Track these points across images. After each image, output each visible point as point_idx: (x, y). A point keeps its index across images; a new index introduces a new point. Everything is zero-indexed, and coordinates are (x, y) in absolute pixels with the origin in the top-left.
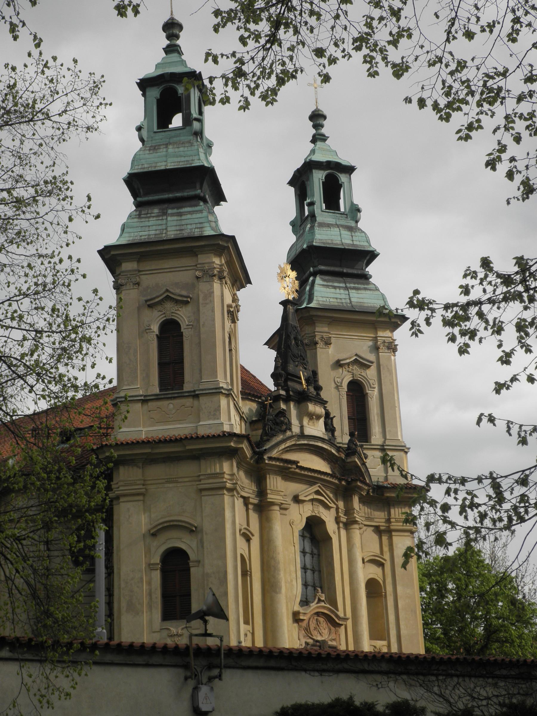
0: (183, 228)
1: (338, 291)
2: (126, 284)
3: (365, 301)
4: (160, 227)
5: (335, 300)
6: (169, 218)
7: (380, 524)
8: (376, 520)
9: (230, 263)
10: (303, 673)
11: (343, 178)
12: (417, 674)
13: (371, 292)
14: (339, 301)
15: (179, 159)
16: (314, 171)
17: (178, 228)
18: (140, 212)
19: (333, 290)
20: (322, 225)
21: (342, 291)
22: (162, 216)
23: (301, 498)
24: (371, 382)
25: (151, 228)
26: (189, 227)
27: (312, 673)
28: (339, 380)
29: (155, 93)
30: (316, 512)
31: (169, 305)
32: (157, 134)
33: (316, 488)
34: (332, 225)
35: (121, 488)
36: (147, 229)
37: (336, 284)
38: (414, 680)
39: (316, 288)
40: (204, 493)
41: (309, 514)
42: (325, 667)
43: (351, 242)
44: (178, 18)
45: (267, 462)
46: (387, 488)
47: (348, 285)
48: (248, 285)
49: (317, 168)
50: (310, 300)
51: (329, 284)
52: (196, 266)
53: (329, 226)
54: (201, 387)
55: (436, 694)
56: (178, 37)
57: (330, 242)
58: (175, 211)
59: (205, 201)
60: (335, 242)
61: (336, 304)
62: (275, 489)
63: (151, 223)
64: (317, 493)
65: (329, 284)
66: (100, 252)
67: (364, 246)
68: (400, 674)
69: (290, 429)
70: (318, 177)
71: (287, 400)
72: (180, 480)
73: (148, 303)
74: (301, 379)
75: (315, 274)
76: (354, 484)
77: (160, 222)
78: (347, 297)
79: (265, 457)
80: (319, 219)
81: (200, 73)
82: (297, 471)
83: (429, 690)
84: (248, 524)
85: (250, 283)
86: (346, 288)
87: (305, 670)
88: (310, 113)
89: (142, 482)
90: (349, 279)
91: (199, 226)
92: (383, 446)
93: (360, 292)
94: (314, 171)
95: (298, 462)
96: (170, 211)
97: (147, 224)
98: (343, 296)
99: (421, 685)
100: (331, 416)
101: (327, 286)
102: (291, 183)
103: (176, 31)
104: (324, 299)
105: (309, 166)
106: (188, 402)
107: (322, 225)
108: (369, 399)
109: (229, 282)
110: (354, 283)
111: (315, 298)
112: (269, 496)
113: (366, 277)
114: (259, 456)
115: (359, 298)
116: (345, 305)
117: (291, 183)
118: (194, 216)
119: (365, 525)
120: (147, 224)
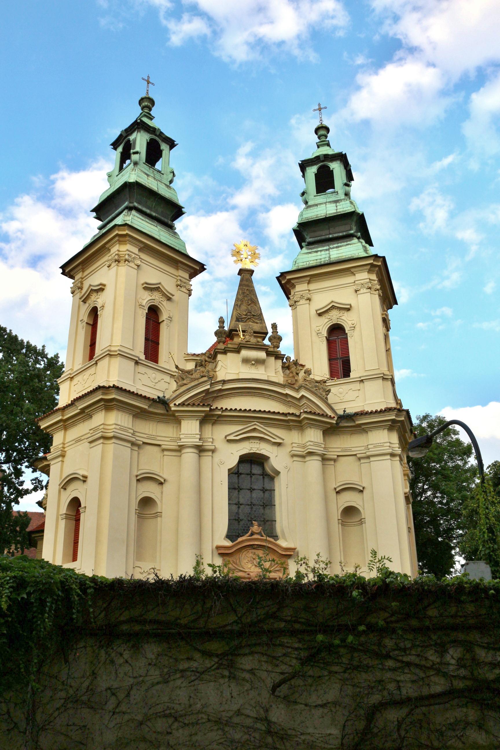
1: (319, 253)
3: (343, 254)
5: (315, 261)
8: (353, 449)
13: (354, 245)
14: (318, 261)
16: (307, 168)
19: (315, 254)
21: (323, 253)
24: (350, 323)
37: (320, 249)
43: (335, 211)
45: (173, 409)
47: (331, 246)
49: (309, 166)
53: (316, 205)
60: (319, 215)
64: (254, 430)
65: (313, 250)
67: (346, 211)
70: (312, 171)
72: (82, 438)
79: (172, 405)
86: (328, 250)
92: (360, 377)
93: (340, 248)
98: (323, 256)
101: (310, 253)
103: (145, 103)
104: (305, 263)
110: (338, 243)
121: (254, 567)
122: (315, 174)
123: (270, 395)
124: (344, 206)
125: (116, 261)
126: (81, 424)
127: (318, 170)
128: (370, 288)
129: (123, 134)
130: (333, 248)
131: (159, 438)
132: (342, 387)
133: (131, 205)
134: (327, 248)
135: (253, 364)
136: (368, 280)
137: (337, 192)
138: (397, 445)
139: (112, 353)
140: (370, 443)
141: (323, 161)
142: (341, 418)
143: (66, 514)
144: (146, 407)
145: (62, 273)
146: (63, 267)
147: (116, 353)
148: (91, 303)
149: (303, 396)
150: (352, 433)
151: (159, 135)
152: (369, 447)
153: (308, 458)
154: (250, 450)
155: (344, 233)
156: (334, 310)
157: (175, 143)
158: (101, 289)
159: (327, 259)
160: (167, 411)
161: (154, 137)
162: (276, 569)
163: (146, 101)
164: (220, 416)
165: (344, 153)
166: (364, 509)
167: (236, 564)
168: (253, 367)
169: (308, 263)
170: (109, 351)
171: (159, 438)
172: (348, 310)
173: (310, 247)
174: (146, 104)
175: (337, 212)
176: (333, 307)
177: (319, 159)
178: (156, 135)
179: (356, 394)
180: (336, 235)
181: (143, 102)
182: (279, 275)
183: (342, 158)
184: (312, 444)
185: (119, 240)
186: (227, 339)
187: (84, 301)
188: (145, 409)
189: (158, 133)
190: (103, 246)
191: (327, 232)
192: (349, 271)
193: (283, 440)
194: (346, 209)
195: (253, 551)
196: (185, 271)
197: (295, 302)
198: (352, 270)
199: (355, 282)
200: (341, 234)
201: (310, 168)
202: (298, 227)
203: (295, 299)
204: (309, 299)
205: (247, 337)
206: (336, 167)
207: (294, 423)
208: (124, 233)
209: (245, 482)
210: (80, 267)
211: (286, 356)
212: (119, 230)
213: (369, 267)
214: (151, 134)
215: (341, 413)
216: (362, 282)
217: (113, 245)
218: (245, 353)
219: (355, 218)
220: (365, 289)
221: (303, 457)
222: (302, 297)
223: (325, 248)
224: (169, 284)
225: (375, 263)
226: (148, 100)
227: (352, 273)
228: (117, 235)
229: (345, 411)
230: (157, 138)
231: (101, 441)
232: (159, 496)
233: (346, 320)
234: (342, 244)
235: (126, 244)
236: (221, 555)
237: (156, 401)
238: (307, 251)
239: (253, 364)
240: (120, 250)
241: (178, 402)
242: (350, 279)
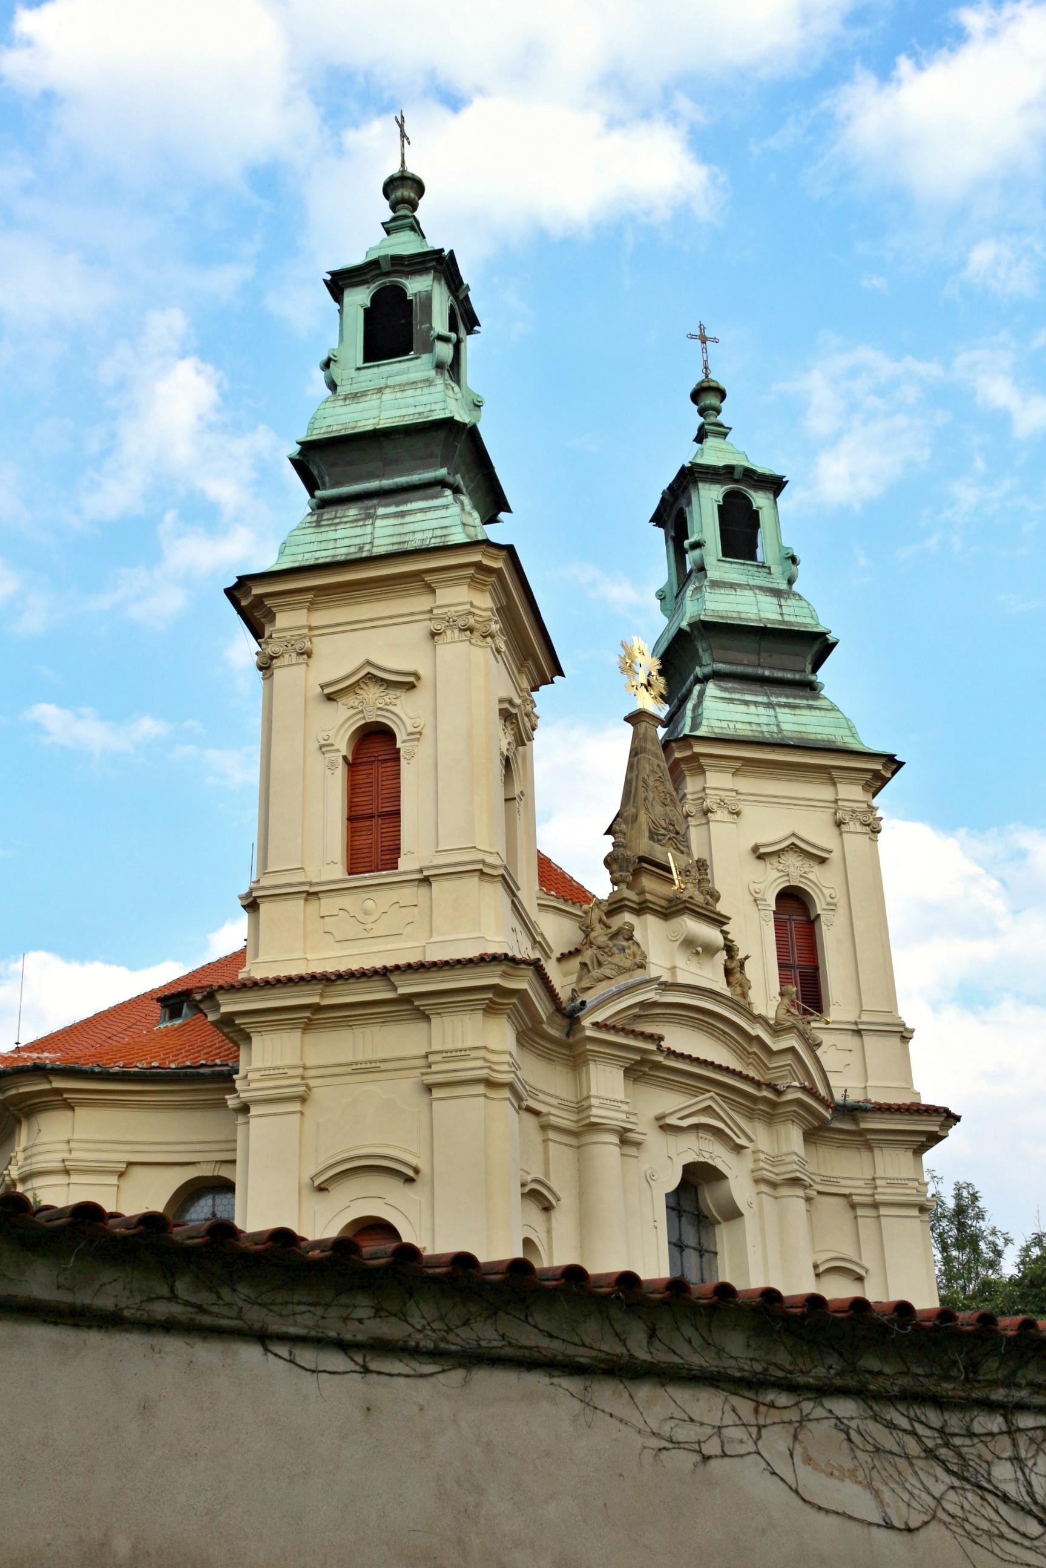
0: (406, 538)
1: (752, 709)
2: (282, 655)
4: (358, 541)
5: (747, 727)
6: (378, 523)
7: (853, 1191)
9: (506, 612)
10: (250, 1354)
11: (759, 500)
12: (911, 1398)
13: (823, 713)
14: (755, 727)
15: (404, 412)
16: (700, 485)
17: (396, 539)
18: (320, 516)
19: (742, 708)
20: (716, 584)
21: (761, 710)
22: (364, 519)
24: (827, 892)
25: (339, 544)
26: (419, 536)
27: (307, 1356)
28: (757, 887)
29: (359, 298)
30: (707, 1155)
31: (372, 694)
32: (363, 372)
33: (704, 1100)
34: (739, 585)
35: (253, 1086)
36: (331, 545)
38: (891, 1426)
39: (707, 703)
40: (437, 1093)
42: (391, 1329)
43: (779, 618)
44: (412, 169)
46: (865, 1110)
47: (774, 699)
48: (557, 679)
49: (705, 481)
50: (695, 725)
51: (733, 696)
52: (431, 611)
53: (732, 586)
54: (436, 862)
55: (1005, 1498)
56: (414, 206)
57: (735, 615)
58: (393, 509)
59: (456, 490)
60: (744, 616)
61: (750, 733)
63: (340, 534)
64: (708, 1110)
65: (733, 696)
66: (228, 592)
67: (805, 625)
68: (822, 1391)
69: (642, 966)
71: (641, 909)
72: (383, 1066)
73: (327, 691)
74: (671, 873)
75: (704, 680)
77: (358, 531)
78: (773, 721)
79: (586, 1022)
80: (713, 574)
81: (452, 252)
82: (660, 1058)
83: (966, 1476)
84: (547, 1173)
85: (562, 674)
86: (769, 705)
87: (263, 1338)
88: (692, 386)
89: (300, 1071)
90: (775, 690)
91: (439, 533)
92: (856, 1023)
93: (798, 712)
94: (700, 485)
95: (661, 1038)
96: (381, 511)
97: (332, 535)
99: (930, 1454)
100: (741, 955)
101: (731, 701)
102: (658, 519)
104: (724, 724)
105: (689, 477)
106: (407, 894)
107: (716, 584)
108: (824, 927)
109: (503, 648)
110: (787, 697)
111: (704, 722)
112: (594, 1111)
113: (811, 688)
114: (571, 1016)
115: (795, 721)
116: (767, 735)
117: (658, 519)
118: (431, 515)
119: (819, 1193)
120: (332, 535)
123: (725, 1033)
124: (797, 611)
126: (376, 1029)
127: (727, 496)
129: (382, 263)
130: (780, 705)
133: (450, 479)
134: (764, 699)
136: (865, 805)
137: (769, 568)
139: (486, 870)
141: (736, 481)
145: (228, 592)
146: (244, 582)
149: (792, 1050)
150: (842, 1145)
153: (783, 1191)
155: (797, 677)
156: (791, 853)
158: (408, 684)
159: (775, 730)
160: (568, 1035)
163: (412, 188)
168: (695, 959)
169: (731, 725)
170: (483, 862)
172: (822, 861)
173: (722, 684)
175: (783, 622)
176: (793, 847)
177: (732, 473)
179: (847, 1058)
180: (778, 674)
181: (402, 186)
185: (472, 578)
189: (461, 297)
190: (416, 576)
191: (753, 658)
192: (828, 775)
194: (800, 620)
198: (834, 773)
199: (836, 801)
200: (789, 676)
201: (707, 486)
203: (708, 803)
204: (738, 814)
205: (689, 885)
207: (768, 1106)
210: (310, 596)
213: (869, 776)
216: (855, 805)
219: (816, 647)
220: (858, 824)
221: (774, 1185)
223: (760, 699)
225: (883, 772)
226: (415, 185)
228: (478, 566)
231: (481, 1089)
232: (543, 1236)
233: (823, 885)
234: (798, 701)
235: (482, 591)
239: (697, 953)
240: (475, 603)
241: (600, 1016)
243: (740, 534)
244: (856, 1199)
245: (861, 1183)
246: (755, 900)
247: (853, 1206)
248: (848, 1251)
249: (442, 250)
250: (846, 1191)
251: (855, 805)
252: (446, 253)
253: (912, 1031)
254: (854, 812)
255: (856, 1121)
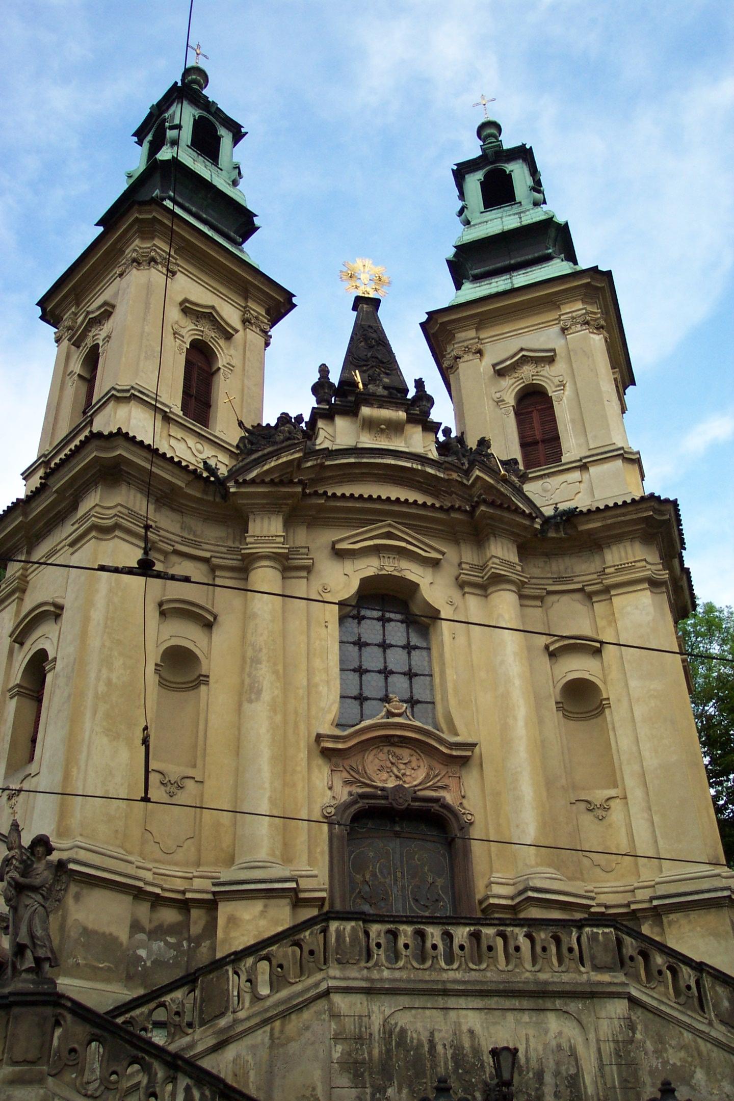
16: (467, 176)
23: (337, 546)
28: (498, 395)
41: (370, 572)
45: (232, 490)
49: (468, 172)
62: (265, 533)
64: (389, 535)
70: (474, 182)
72: (58, 548)
76: (478, 513)
92: (580, 460)
121: (393, 778)
122: (482, 183)
125: (134, 260)
128: (587, 323)
131: (205, 546)
132: (548, 480)
135: (382, 431)
138: (661, 567)
139: (118, 395)
140: (607, 565)
142: (547, 520)
143: (18, 685)
144: (183, 485)
145: (42, 318)
147: (128, 395)
148: (89, 342)
151: (215, 112)
152: (607, 571)
154: (381, 569)
157: (243, 130)
161: (205, 114)
162: (439, 784)
164: (321, 509)
165: (528, 147)
166: (605, 683)
167: (358, 773)
171: (205, 546)
172: (551, 360)
174: (194, 77)
176: (525, 360)
178: (209, 112)
182: (424, 318)
183: (524, 154)
184: (497, 561)
186: (335, 398)
187: (77, 344)
188: (181, 488)
189: (213, 110)
193: (443, 554)
195: (389, 748)
196: (258, 301)
197: (457, 357)
202: (454, 256)
206: (518, 171)
208: (150, 217)
209: (371, 631)
211: (442, 427)
212: (140, 212)
214: (201, 109)
215: (548, 511)
217: (128, 243)
218: (366, 411)
219: (552, 233)
222: (467, 350)
224: (231, 314)
227: (555, 304)
229: (556, 509)
230: (211, 117)
236: (327, 754)
237: (200, 476)
238: (471, 286)
242: (553, 315)
243: (498, 192)
244: (588, 589)
245: (595, 576)
246: (497, 402)
247: (589, 596)
248: (587, 631)
249: (176, 83)
250: (579, 586)
251: (574, 314)
252: (179, 84)
253: (638, 453)
254: (573, 318)
255: (576, 527)
